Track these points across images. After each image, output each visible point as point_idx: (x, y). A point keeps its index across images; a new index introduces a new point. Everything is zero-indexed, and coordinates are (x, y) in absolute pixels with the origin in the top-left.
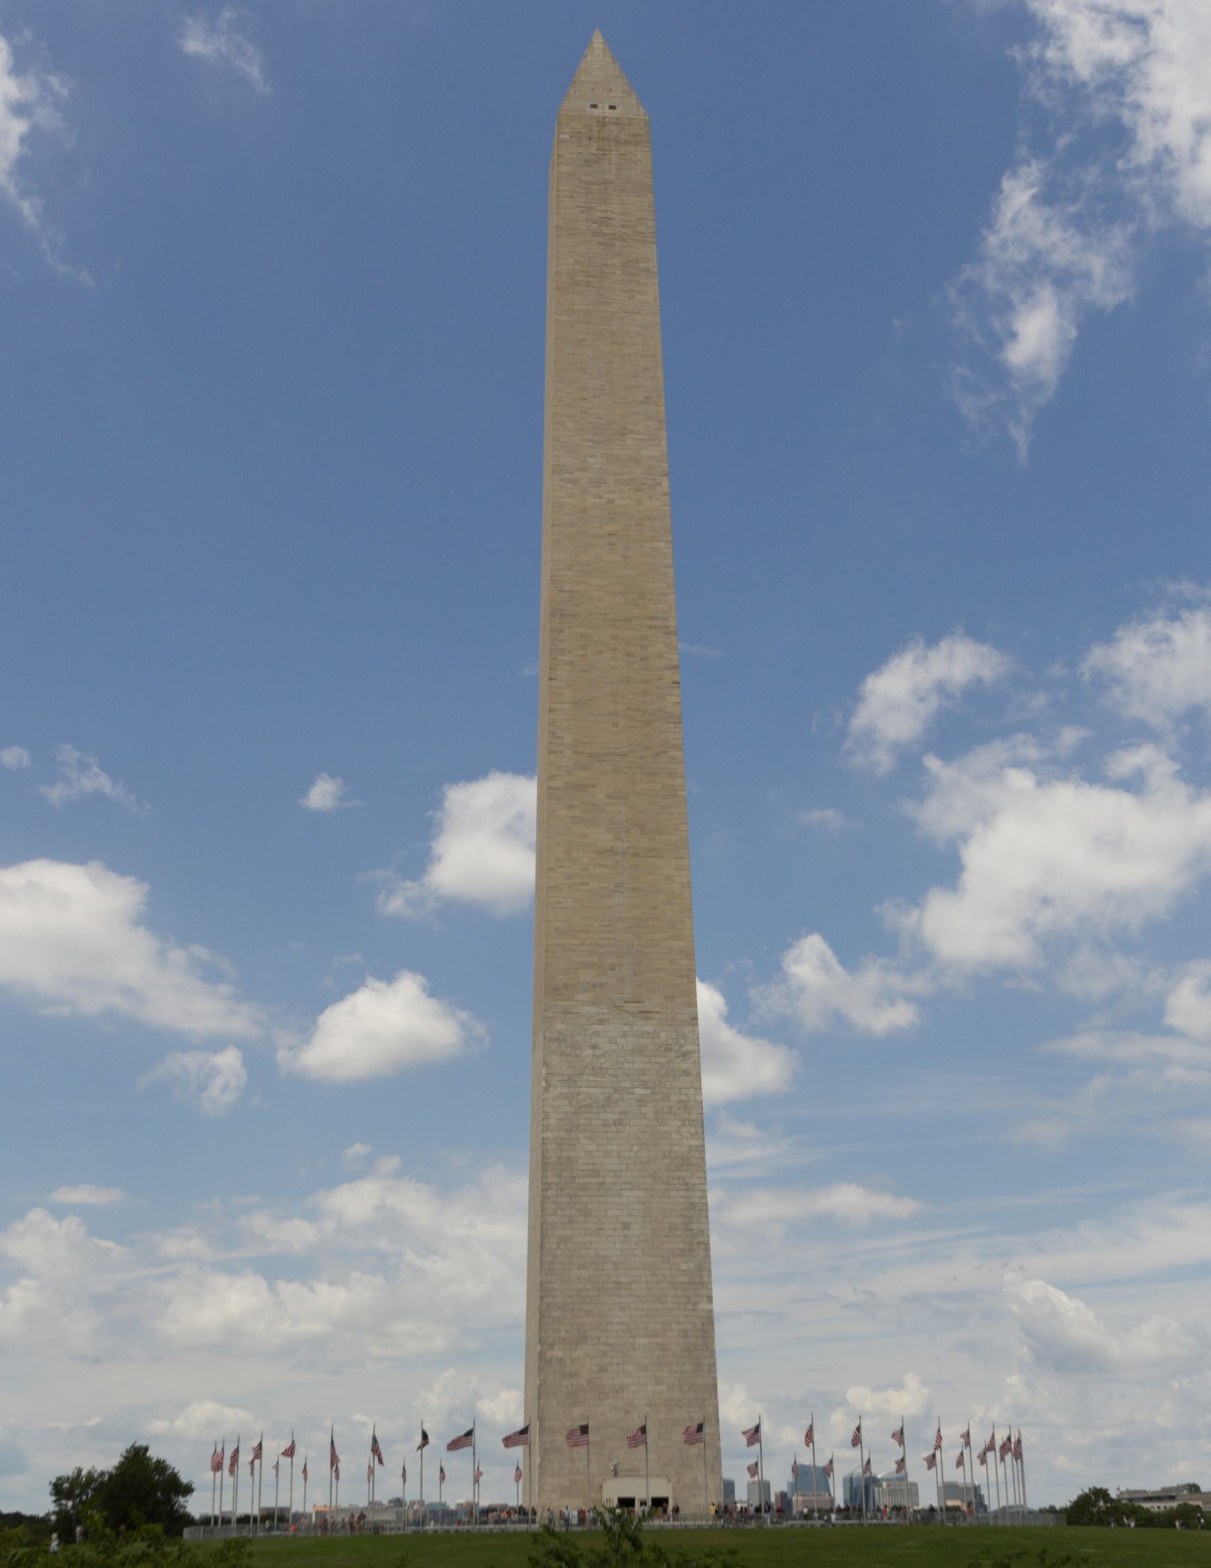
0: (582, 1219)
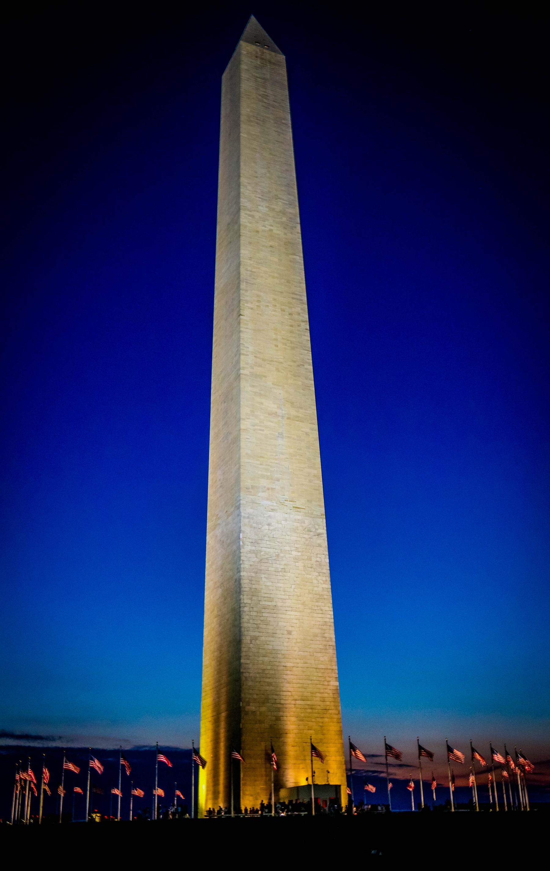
0: (264, 626)
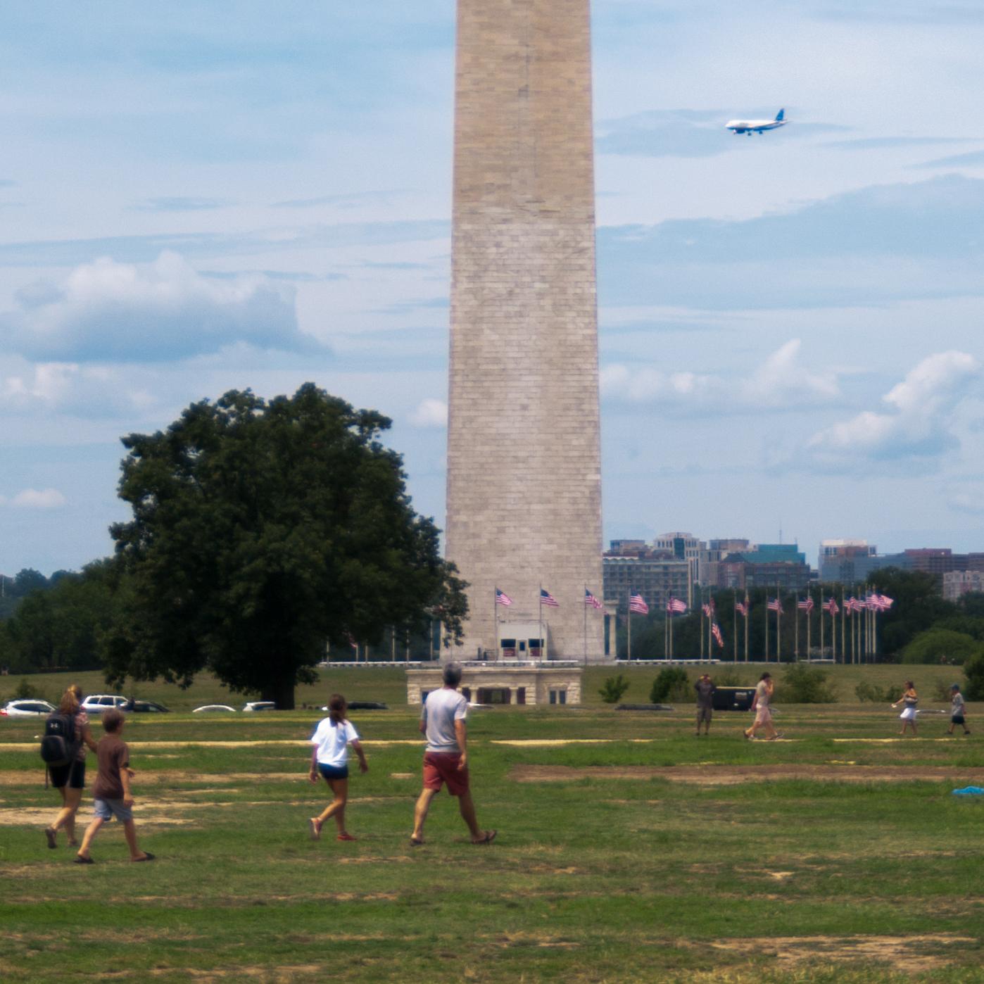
0: (485, 401)
